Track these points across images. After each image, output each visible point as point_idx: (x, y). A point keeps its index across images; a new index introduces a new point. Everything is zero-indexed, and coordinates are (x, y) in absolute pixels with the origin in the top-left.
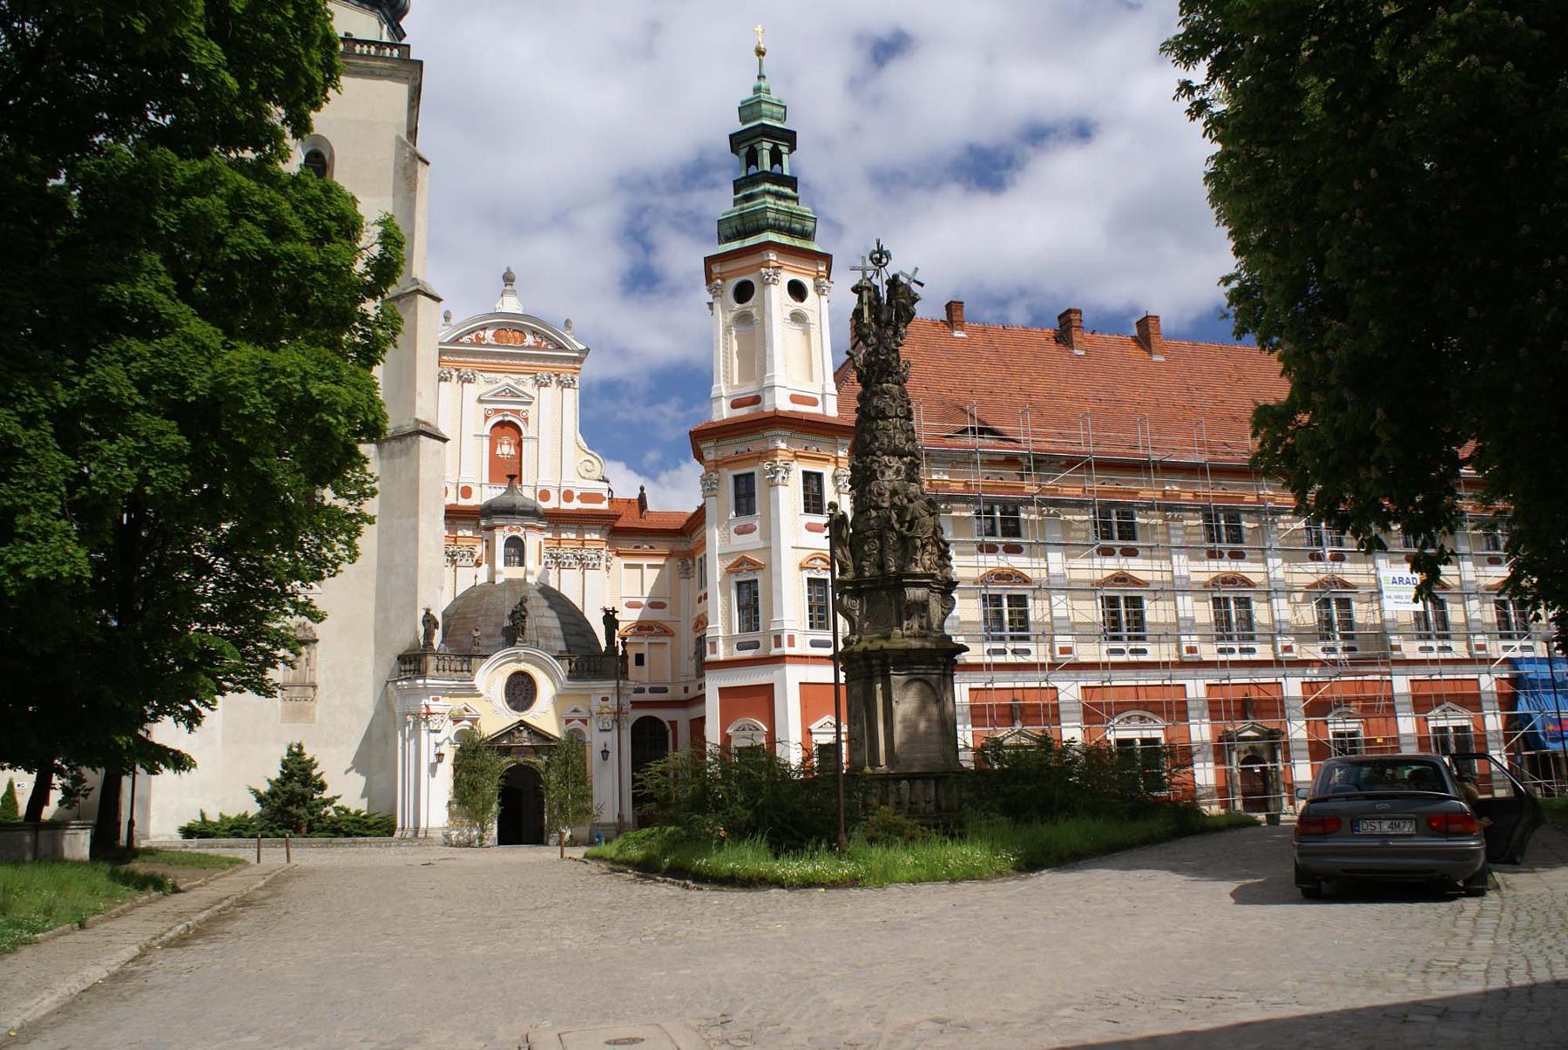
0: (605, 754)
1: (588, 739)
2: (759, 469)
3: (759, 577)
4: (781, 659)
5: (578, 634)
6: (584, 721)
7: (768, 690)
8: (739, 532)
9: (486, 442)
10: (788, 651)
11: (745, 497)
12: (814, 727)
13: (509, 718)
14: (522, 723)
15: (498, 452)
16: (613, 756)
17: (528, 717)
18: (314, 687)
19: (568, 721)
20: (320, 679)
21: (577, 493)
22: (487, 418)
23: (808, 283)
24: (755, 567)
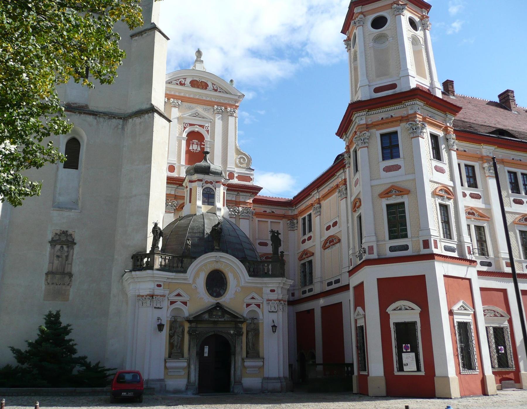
0: (274, 327)
1: (261, 317)
2: (401, 129)
3: (405, 199)
4: (431, 256)
5: (250, 249)
6: (258, 306)
7: (421, 279)
8: (388, 169)
9: (184, 143)
10: (435, 251)
11: (390, 147)
12: (455, 308)
13: (208, 300)
14: (218, 305)
15: (191, 148)
16: (279, 330)
17: (222, 300)
18: (70, 275)
19: (248, 305)
20: (75, 269)
21: (236, 175)
22: (185, 128)
23: (417, 19)
24: (402, 191)
